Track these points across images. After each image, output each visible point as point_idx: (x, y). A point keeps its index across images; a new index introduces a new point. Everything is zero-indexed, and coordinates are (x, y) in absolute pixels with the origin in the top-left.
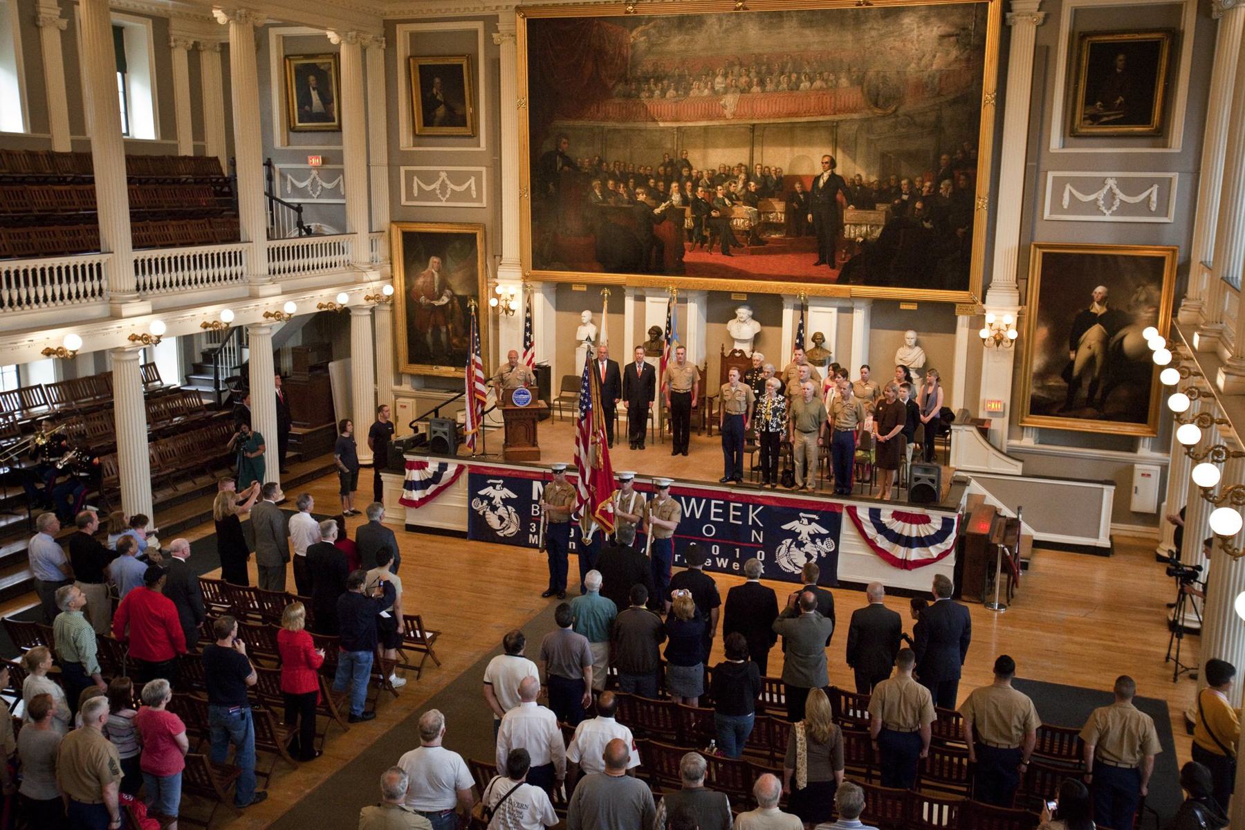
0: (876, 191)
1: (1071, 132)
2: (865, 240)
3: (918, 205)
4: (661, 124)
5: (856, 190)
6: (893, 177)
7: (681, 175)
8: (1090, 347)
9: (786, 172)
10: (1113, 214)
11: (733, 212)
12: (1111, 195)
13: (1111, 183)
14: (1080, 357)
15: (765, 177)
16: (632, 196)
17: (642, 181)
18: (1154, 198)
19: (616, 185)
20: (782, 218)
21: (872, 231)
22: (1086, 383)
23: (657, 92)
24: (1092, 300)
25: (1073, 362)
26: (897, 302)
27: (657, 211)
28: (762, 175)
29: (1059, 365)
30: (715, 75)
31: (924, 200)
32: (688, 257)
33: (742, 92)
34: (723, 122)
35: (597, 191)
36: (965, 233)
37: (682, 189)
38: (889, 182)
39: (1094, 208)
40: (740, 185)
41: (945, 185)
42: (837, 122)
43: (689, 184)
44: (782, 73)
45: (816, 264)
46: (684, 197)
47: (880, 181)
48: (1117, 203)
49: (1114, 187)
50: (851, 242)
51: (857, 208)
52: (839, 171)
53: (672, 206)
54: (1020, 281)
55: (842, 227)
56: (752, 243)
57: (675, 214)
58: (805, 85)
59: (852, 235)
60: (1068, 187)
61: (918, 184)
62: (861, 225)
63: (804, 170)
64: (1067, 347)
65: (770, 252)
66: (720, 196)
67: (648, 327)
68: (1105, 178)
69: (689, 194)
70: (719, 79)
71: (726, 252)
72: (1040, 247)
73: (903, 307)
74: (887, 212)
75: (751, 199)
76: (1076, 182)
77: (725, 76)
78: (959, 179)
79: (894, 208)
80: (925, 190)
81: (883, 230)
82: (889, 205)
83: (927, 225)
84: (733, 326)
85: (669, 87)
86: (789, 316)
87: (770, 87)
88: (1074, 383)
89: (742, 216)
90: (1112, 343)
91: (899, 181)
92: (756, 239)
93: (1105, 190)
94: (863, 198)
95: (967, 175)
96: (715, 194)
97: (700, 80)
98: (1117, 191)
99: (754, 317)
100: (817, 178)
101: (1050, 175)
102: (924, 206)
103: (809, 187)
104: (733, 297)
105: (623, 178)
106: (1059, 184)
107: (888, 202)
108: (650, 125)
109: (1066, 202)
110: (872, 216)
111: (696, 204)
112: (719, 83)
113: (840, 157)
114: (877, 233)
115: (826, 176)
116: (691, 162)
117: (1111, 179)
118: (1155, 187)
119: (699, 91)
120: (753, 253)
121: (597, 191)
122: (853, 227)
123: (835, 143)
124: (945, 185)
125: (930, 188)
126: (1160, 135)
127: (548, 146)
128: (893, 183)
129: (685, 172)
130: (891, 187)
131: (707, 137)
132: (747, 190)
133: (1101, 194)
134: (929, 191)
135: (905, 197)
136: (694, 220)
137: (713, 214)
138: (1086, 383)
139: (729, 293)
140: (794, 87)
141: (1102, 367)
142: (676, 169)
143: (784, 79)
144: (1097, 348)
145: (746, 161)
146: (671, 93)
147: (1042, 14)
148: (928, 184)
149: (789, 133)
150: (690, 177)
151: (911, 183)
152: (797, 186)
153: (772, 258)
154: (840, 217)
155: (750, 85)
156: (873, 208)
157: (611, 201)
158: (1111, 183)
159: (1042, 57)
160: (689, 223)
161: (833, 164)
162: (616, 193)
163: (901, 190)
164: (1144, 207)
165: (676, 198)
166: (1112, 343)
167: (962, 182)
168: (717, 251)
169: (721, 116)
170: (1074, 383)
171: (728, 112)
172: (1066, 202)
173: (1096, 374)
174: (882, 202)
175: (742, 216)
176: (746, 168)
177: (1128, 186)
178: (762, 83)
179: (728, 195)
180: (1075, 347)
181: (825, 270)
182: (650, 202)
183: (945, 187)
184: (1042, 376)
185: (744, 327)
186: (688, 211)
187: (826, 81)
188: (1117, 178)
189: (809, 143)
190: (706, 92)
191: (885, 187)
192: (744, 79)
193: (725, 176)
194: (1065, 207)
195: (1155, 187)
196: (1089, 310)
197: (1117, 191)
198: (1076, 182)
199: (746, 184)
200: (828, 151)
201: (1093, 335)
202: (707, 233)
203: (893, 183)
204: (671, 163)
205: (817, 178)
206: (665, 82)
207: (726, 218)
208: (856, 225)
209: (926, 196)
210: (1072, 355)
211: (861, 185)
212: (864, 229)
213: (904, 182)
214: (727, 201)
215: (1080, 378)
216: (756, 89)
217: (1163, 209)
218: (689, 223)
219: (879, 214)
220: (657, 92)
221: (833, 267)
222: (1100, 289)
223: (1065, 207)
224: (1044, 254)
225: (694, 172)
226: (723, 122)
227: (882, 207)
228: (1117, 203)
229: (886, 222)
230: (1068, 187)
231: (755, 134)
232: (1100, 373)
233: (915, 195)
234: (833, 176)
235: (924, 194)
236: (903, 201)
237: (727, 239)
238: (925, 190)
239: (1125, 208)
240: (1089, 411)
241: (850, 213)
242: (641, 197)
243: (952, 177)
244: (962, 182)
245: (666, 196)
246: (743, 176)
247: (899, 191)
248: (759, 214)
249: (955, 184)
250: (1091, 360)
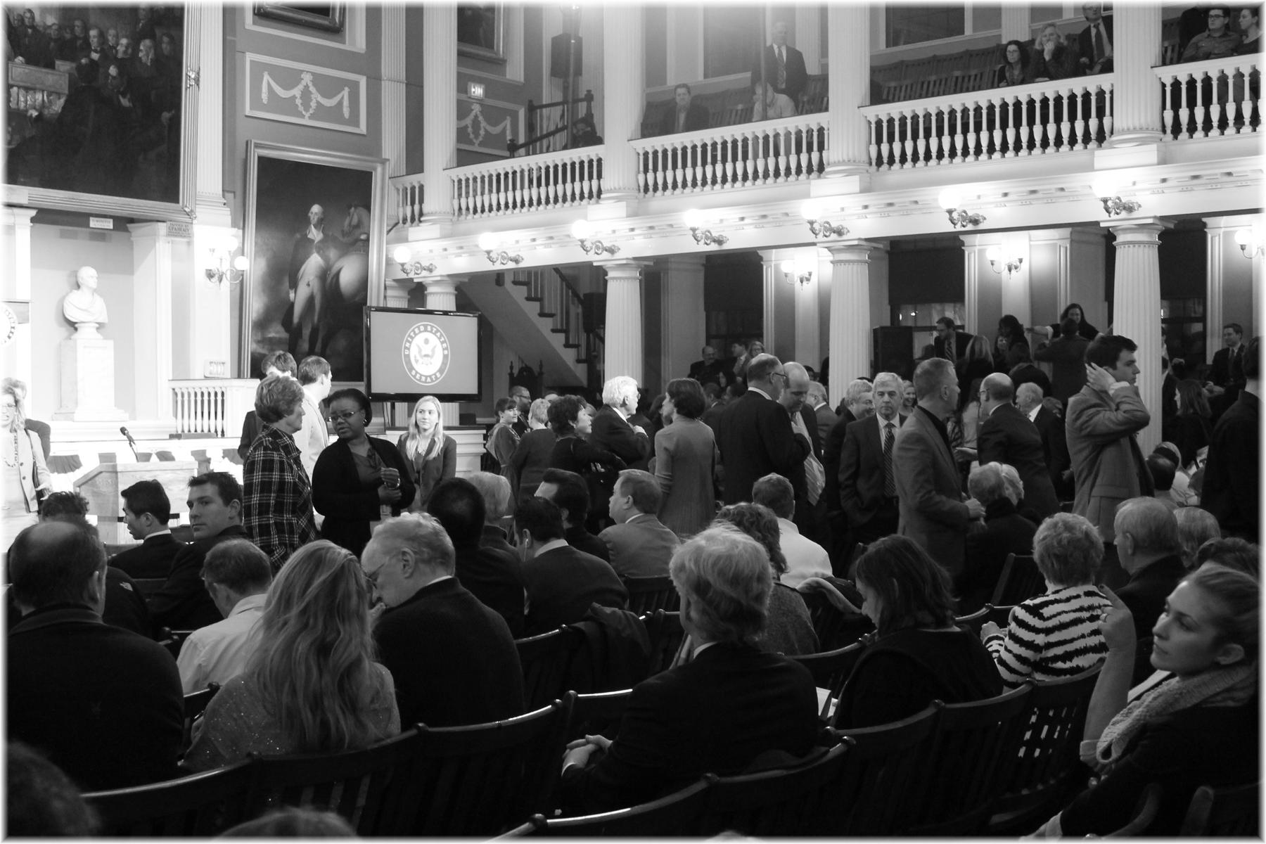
0: (56, 41)
2: (40, 116)
3: (113, 71)
5: (26, 35)
6: (78, 23)
8: (308, 285)
10: (310, 118)
12: (306, 94)
13: (307, 78)
14: (299, 297)
18: (346, 103)
21: (50, 102)
22: (306, 332)
24: (307, 222)
25: (292, 305)
26: (86, 216)
29: (279, 311)
31: (121, 64)
36: (171, 119)
38: (72, 29)
39: (287, 106)
41: (145, 45)
47: (61, 28)
48: (313, 104)
49: (310, 84)
51: (29, 62)
54: (227, 194)
59: (22, 105)
60: (266, 77)
61: (111, 41)
62: (34, 90)
64: (287, 284)
68: (302, 71)
72: (257, 146)
73: (94, 223)
74: (70, 75)
76: (274, 71)
78: (161, 42)
79: (80, 68)
80: (121, 49)
81: (66, 101)
82: (74, 65)
83: (125, 102)
90: (329, 280)
91: (86, 29)
93: (301, 87)
95: (172, 39)
98: (312, 89)
101: (250, 57)
102: (120, 73)
106: (258, 68)
107: (72, 59)
109: (265, 96)
114: (58, 105)
117: (308, 72)
118: (347, 89)
122: (22, 92)
124: (145, 45)
125: (127, 47)
128: (78, 31)
130: (76, 38)
133: (297, 92)
134: (125, 52)
135: (95, 56)
138: (306, 332)
141: (321, 307)
144: (316, 286)
148: (124, 41)
151: (102, 35)
156: (50, 65)
158: (307, 78)
163: (89, 45)
164: (334, 113)
166: (329, 280)
167: (166, 47)
172: (265, 96)
173: (316, 318)
174: (64, 58)
177: (328, 87)
180: (294, 285)
184: (262, 324)
188: (313, 74)
191: (68, 36)
194: (265, 101)
195: (347, 89)
196: (306, 235)
197: (312, 89)
198: (274, 71)
203: (78, 31)
208: (27, 89)
209: (121, 59)
210: (292, 295)
211: (33, 27)
212: (39, 96)
213: (93, 33)
215: (300, 326)
217: (354, 121)
222: (316, 209)
223: (265, 101)
224: (261, 159)
227: (63, 66)
228: (313, 104)
229: (70, 86)
230: (266, 77)
232: (319, 320)
233: (108, 54)
235: (120, 55)
236: (92, 61)
238: (121, 49)
239: (321, 112)
243: (152, 36)
244: (166, 47)
249: (157, 46)
250: (311, 300)
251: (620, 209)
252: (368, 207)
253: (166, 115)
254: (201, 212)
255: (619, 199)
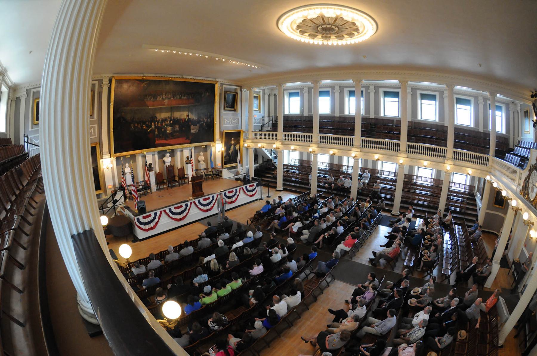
1: (224, 110)
3: (205, 124)
4: (150, 107)
7: (154, 120)
9: (178, 118)
11: (167, 129)
14: (230, 152)
15: (174, 119)
16: (142, 127)
17: (144, 123)
19: (138, 124)
20: (178, 129)
22: (232, 157)
23: (149, 99)
24: (231, 140)
26: (201, 146)
27: (149, 131)
28: (174, 119)
30: (163, 95)
32: (157, 142)
33: (169, 99)
34: (164, 106)
35: (132, 127)
37: (155, 125)
40: (169, 122)
42: (189, 106)
43: (156, 123)
44: (178, 95)
45: (186, 140)
46: (155, 127)
50: (192, 133)
51: (193, 125)
52: (190, 117)
53: (152, 129)
55: (191, 130)
56: (172, 136)
57: (153, 131)
58: (183, 98)
61: (204, 120)
63: (182, 118)
65: (177, 138)
66: (164, 125)
67: (148, 163)
69: (156, 125)
70: (164, 96)
71: (166, 140)
75: (171, 125)
77: (165, 95)
84: (165, 159)
85: (152, 98)
86: (178, 154)
87: (175, 98)
88: (230, 157)
89: (169, 130)
91: (201, 119)
92: (172, 136)
94: (194, 123)
96: (163, 125)
97: (159, 96)
99: (170, 156)
100: (186, 119)
101: (223, 117)
103: (184, 121)
104: (168, 151)
105: (139, 123)
108: (147, 107)
110: (196, 127)
111: (159, 128)
112: (164, 97)
113: (190, 114)
114: (197, 131)
115: (187, 119)
116: (157, 117)
119: (159, 99)
120: (172, 139)
121: (132, 127)
123: (189, 112)
126: (235, 110)
127: (118, 116)
129: (155, 119)
131: (161, 110)
132: (171, 124)
135: (202, 122)
136: (158, 132)
137: (162, 130)
139: (166, 150)
140: (180, 98)
142: (153, 119)
143: (178, 96)
145: (170, 116)
146: (152, 99)
147: (221, 87)
149: (178, 109)
150: (157, 121)
151: (203, 119)
152: (181, 121)
153: (176, 140)
154: (190, 127)
155: (171, 97)
157: (136, 130)
159: (220, 94)
160: (156, 133)
161: (188, 116)
162: (138, 127)
165: (153, 127)
168: (164, 139)
169: (164, 105)
170: (230, 157)
171: (166, 104)
175: (169, 130)
176: (170, 118)
177: (234, 119)
178: (173, 97)
179: (166, 125)
181: (188, 141)
182: (147, 129)
183: (209, 120)
184: (225, 157)
185: (168, 159)
186: (156, 130)
187: (187, 97)
189: (184, 111)
190: (161, 99)
192: (169, 96)
193: (165, 120)
199: (170, 122)
200: (187, 113)
201: (232, 147)
202: (161, 135)
204: (152, 117)
205: (186, 119)
206: (151, 96)
207: (166, 131)
214: (166, 126)
216: (172, 98)
218: (156, 133)
219: (197, 127)
220: (149, 99)
221: (189, 140)
222: (233, 138)
225: (158, 119)
226: (164, 106)
227: (198, 125)
231: (172, 109)
234: (188, 118)
237: (165, 136)
239: (233, 123)
240: (232, 162)
241: (192, 127)
242: (144, 127)
245: (151, 126)
246: (169, 120)
247: (201, 121)
248: (173, 129)
250: (232, 152)
251: (280, 143)
252: (240, 137)
253: (212, 129)
254: (217, 142)
255: (280, 141)
